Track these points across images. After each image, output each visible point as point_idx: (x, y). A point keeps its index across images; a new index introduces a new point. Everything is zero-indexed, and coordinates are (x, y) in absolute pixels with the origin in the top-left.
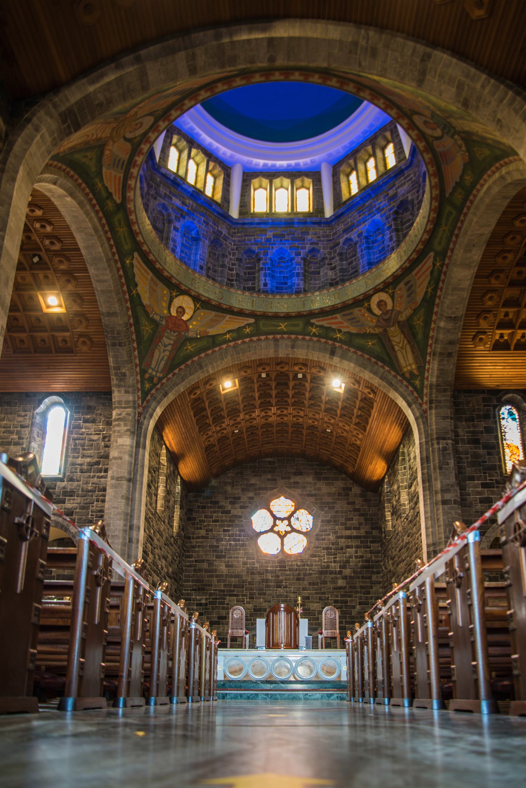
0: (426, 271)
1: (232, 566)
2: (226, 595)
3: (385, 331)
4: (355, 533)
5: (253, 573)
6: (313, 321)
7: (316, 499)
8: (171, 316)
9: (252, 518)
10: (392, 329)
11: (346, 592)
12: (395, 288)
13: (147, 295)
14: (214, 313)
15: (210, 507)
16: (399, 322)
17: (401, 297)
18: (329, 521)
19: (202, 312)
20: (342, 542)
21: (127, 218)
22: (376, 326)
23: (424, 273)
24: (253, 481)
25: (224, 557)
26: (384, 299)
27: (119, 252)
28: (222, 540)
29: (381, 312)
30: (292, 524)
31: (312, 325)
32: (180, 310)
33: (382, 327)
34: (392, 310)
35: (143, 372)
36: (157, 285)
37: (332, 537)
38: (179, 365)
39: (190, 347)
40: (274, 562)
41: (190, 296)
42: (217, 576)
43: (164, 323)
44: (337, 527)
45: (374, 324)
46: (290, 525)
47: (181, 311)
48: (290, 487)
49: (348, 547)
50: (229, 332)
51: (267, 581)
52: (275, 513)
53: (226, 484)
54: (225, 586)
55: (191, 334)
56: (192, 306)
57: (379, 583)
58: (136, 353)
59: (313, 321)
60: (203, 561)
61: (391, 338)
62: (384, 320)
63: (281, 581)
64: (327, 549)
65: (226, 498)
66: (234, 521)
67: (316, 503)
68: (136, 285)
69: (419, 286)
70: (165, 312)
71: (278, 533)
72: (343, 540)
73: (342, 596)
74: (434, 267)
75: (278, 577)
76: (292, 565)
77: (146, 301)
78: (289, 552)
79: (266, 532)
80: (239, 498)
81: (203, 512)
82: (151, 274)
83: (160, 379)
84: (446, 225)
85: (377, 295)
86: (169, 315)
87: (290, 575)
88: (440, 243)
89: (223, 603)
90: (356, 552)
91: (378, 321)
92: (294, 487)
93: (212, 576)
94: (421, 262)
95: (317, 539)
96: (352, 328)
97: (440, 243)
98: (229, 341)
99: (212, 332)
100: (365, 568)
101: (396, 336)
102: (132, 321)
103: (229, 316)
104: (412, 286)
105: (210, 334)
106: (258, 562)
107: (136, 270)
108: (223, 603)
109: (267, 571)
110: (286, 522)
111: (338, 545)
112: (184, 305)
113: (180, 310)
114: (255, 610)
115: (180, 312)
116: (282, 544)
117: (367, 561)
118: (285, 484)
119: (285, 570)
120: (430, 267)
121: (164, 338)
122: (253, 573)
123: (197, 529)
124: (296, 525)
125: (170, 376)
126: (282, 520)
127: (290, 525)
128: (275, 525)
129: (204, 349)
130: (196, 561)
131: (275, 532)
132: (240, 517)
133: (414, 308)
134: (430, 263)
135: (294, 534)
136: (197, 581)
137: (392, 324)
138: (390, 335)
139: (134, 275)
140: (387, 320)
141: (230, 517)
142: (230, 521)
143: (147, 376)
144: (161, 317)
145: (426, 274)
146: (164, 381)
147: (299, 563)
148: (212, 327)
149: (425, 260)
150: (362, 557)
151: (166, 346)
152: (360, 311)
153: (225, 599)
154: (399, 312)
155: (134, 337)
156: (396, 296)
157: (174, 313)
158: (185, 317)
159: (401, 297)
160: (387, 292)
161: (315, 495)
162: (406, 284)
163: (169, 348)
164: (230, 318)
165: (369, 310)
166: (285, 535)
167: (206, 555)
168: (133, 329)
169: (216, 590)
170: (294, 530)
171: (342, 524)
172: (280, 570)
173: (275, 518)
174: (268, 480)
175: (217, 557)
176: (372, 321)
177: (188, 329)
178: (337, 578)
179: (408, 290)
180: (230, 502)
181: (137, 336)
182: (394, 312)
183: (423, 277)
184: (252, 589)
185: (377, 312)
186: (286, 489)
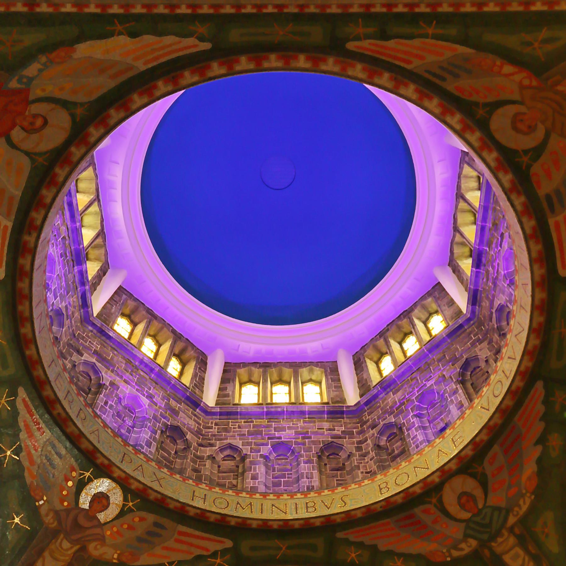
0: (198, 547)
3: (55, 534)
6: (22, 393)
8: (27, 103)
10: (66, 544)
12: (139, 509)
14: (18, 194)
16: (83, 549)
17: (131, 528)
21: (302, 49)
22: (57, 513)
23: (191, 545)
26: (112, 500)
29: (86, 506)
31: (13, 393)
32: (39, 122)
33: (60, 522)
34: (102, 525)
41: (67, 144)
45: (58, 507)
59: (22, 393)
61: (46, 554)
62: (75, 521)
68: (133, 35)
69: (167, 549)
74: (209, 556)
82: (143, 68)
84: (288, 548)
85: (114, 485)
86: (31, 97)
88: (253, 548)
91: (68, 511)
94: (206, 532)
96: (34, 469)
97: (253, 548)
101: (56, 559)
103: (10, 225)
104: (158, 535)
107: (169, 39)
112: (47, 131)
115: (32, 124)
120: (208, 550)
133: (124, 559)
134: (213, 547)
137: (74, 537)
138: (52, 547)
139: (160, 34)
140: (76, 525)
144: (31, 80)
145: (193, 549)
149: (212, 537)
152: (73, 469)
154: (102, 540)
156: (128, 518)
158: (17, 134)
159: (131, 528)
160: (125, 499)
162: (156, 524)
164: (6, 227)
165: (81, 485)
176: (62, 502)
179: (150, 533)
182: (97, 531)
183: (184, 547)
185: (85, 502)
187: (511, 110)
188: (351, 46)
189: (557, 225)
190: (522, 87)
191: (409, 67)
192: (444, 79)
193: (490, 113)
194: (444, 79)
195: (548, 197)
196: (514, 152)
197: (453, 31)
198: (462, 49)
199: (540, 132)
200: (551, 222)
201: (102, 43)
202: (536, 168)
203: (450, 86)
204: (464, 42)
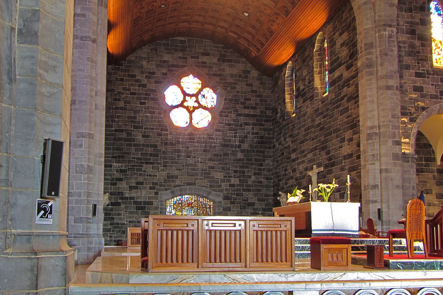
1: (148, 136)
2: (143, 163)
4: (252, 112)
5: (166, 144)
7: (221, 79)
9: (165, 93)
11: (243, 163)
15: (128, 80)
18: (231, 100)
20: (242, 119)
24: (166, 57)
25: (141, 127)
28: (138, 111)
30: (199, 100)
37: (233, 116)
40: (184, 134)
42: (135, 145)
44: (237, 106)
46: (197, 101)
48: (198, 66)
49: (246, 124)
51: (179, 151)
52: (185, 89)
53: (142, 58)
54: (142, 154)
57: (270, 157)
60: (122, 131)
63: (191, 152)
64: (229, 124)
65: (142, 73)
66: (149, 95)
67: (221, 83)
71: (187, 108)
72: (242, 118)
73: (241, 167)
75: (188, 148)
76: (199, 138)
78: (197, 126)
79: (177, 106)
80: (154, 73)
81: (122, 85)
87: (198, 146)
89: (141, 170)
90: (253, 129)
92: (202, 67)
93: (130, 145)
95: (221, 116)
100: (259, 143)
106: (171, 134)
108: (141, 170)
109: (178, 142)
110: (194, 99)
111: (238, 122)
114: (168, 177)
116: (191, 118)
117: (262, 137)
118: (194, 63)
119: (194, 142)
122: (166, 144)
123: (116, 100)
124: (203, 102)
126: (191, 96)
127: (197, 101)
128: (184, 100)
130: (116, 131)
131: (184, 107)
132: (155, 91)
135: (201, 110)
136: (118, 149)
141: (145, 91)
142: (146, 94)
147: (206, 136)
150: (257, 133)
153: (142, 166)
161: (220, 75)
166: (193, 111)
167: (126, 125)
169: (134, 158)
170: (200, 106)
171: (242, 103)
172: (189, 142)
173: (185, 94)
174: (180, 58)
175: (135, 127)
178: (237, 151)
180: (146, 76)
184: (165, 158)
186: (195, 67)
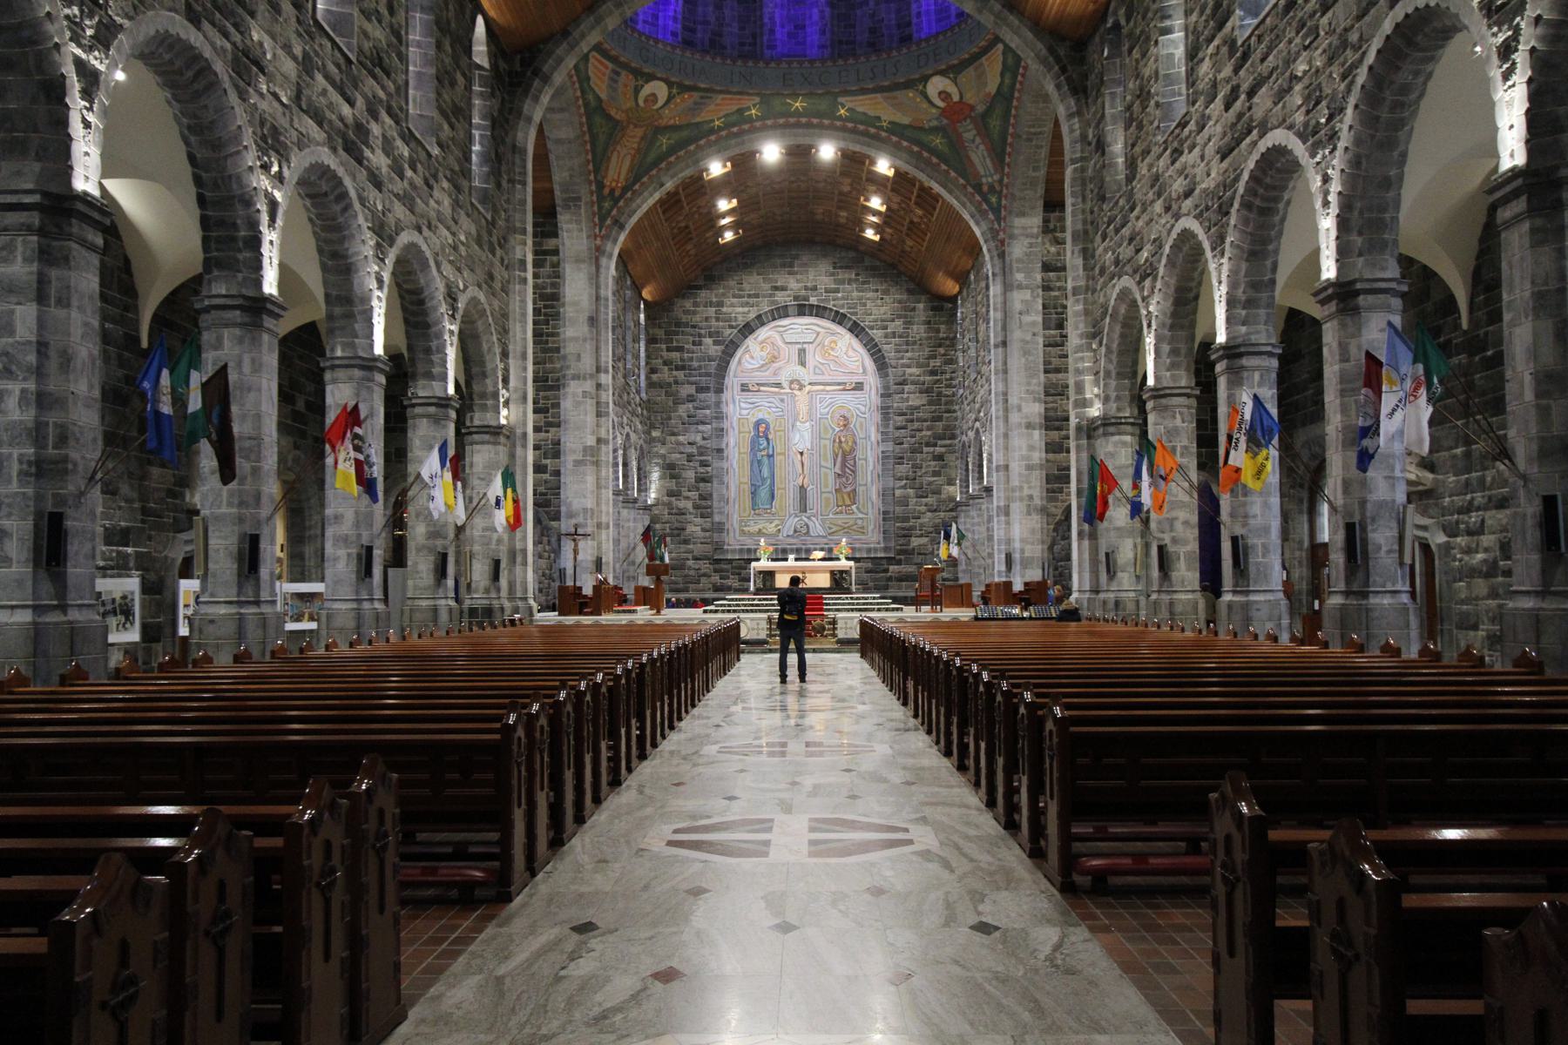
13: (899, 114)
19: (962, 78)
27: (820, 115)
35: (978, 188)
36: (895, 98)
38: (1004, 151)
39: (995, 123)
43: (945, 121)
47: (944, 95)
50: (1002, 75)
55: (980, 108)
56: (947, 81)
58: (953, 174)
68: (878, 118)
70: (934, 111)
77: (906, 121)
82: (878, 95)
83: (1001, 181)
98: (1014, 84)
99: (992, 87)
102: (916, 149)
105: (993, 91)
107: (860, 109)
112: (941, 88)
113: (943, 96)
121: (965, 135)
125: (1006, 170)
129: (1006, 116)
139: (865, 114)
143: (985, 188)
146: (1006, 180)
148: (986, 84)
151: (973, 141)
155: (935, 160)
157: (941, 104)
158: (956, 98)
163: (978, 140)
168: (925, 154)
177: (972, 108)
181: (938, 157)
187: (660, 103)
188: (757, 99)
189: (607, 68)
190: (661, 118)
191: (721, 96)
192: (702, 97)
193: (670, 93)
194: (702, 97)
195: (618, 74)
196: (647, 82)
197: (706, 127)
198: (698, 120)
199: (641, 102)
200: (610, 65)
201: (897, 120)
202: (633, 83)
203: (696, 95)
204: (697, 124)
